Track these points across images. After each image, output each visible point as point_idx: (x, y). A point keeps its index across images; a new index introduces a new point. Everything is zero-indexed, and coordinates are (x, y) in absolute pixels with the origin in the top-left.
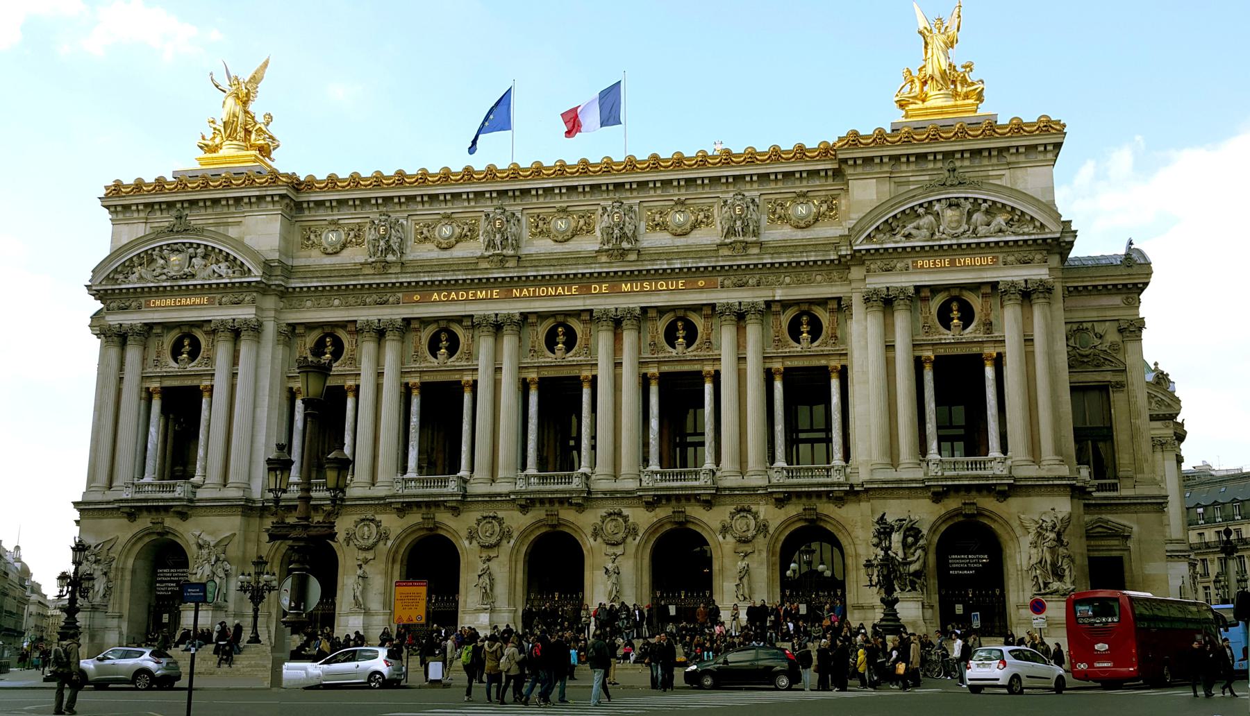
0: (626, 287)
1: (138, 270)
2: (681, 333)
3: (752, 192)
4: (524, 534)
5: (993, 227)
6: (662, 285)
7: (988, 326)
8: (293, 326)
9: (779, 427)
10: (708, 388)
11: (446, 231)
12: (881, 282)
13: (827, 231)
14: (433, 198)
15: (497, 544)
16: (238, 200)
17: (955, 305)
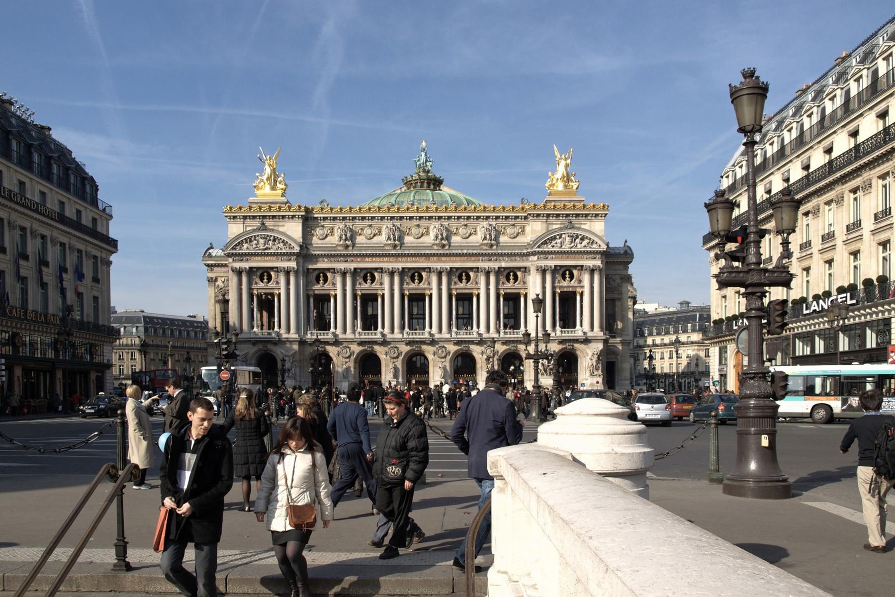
0: (444, 259)
1: (245, 246)
2: (464, 277)
3: (494, 223)
4: (406, 354)
5: (583, 244)
6: (458, 259)
7: (580, 281)
8: (308, 269)
9: (502, 315)
10: (475, 299)
11: (369, 232)
12: (543, 263)
13: (521, 240)
14: (363, 218)
15: (397, 357)
16: (283, 217)
17: (566, 272)
